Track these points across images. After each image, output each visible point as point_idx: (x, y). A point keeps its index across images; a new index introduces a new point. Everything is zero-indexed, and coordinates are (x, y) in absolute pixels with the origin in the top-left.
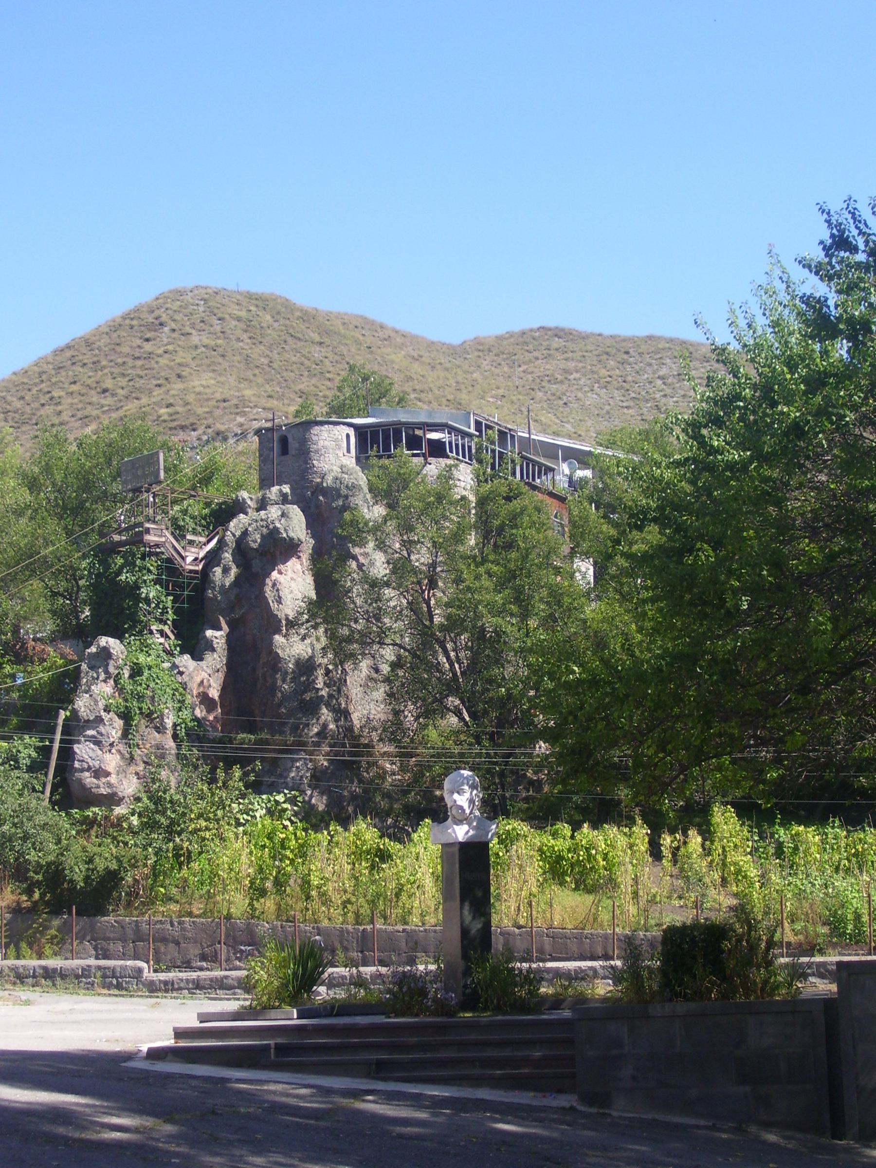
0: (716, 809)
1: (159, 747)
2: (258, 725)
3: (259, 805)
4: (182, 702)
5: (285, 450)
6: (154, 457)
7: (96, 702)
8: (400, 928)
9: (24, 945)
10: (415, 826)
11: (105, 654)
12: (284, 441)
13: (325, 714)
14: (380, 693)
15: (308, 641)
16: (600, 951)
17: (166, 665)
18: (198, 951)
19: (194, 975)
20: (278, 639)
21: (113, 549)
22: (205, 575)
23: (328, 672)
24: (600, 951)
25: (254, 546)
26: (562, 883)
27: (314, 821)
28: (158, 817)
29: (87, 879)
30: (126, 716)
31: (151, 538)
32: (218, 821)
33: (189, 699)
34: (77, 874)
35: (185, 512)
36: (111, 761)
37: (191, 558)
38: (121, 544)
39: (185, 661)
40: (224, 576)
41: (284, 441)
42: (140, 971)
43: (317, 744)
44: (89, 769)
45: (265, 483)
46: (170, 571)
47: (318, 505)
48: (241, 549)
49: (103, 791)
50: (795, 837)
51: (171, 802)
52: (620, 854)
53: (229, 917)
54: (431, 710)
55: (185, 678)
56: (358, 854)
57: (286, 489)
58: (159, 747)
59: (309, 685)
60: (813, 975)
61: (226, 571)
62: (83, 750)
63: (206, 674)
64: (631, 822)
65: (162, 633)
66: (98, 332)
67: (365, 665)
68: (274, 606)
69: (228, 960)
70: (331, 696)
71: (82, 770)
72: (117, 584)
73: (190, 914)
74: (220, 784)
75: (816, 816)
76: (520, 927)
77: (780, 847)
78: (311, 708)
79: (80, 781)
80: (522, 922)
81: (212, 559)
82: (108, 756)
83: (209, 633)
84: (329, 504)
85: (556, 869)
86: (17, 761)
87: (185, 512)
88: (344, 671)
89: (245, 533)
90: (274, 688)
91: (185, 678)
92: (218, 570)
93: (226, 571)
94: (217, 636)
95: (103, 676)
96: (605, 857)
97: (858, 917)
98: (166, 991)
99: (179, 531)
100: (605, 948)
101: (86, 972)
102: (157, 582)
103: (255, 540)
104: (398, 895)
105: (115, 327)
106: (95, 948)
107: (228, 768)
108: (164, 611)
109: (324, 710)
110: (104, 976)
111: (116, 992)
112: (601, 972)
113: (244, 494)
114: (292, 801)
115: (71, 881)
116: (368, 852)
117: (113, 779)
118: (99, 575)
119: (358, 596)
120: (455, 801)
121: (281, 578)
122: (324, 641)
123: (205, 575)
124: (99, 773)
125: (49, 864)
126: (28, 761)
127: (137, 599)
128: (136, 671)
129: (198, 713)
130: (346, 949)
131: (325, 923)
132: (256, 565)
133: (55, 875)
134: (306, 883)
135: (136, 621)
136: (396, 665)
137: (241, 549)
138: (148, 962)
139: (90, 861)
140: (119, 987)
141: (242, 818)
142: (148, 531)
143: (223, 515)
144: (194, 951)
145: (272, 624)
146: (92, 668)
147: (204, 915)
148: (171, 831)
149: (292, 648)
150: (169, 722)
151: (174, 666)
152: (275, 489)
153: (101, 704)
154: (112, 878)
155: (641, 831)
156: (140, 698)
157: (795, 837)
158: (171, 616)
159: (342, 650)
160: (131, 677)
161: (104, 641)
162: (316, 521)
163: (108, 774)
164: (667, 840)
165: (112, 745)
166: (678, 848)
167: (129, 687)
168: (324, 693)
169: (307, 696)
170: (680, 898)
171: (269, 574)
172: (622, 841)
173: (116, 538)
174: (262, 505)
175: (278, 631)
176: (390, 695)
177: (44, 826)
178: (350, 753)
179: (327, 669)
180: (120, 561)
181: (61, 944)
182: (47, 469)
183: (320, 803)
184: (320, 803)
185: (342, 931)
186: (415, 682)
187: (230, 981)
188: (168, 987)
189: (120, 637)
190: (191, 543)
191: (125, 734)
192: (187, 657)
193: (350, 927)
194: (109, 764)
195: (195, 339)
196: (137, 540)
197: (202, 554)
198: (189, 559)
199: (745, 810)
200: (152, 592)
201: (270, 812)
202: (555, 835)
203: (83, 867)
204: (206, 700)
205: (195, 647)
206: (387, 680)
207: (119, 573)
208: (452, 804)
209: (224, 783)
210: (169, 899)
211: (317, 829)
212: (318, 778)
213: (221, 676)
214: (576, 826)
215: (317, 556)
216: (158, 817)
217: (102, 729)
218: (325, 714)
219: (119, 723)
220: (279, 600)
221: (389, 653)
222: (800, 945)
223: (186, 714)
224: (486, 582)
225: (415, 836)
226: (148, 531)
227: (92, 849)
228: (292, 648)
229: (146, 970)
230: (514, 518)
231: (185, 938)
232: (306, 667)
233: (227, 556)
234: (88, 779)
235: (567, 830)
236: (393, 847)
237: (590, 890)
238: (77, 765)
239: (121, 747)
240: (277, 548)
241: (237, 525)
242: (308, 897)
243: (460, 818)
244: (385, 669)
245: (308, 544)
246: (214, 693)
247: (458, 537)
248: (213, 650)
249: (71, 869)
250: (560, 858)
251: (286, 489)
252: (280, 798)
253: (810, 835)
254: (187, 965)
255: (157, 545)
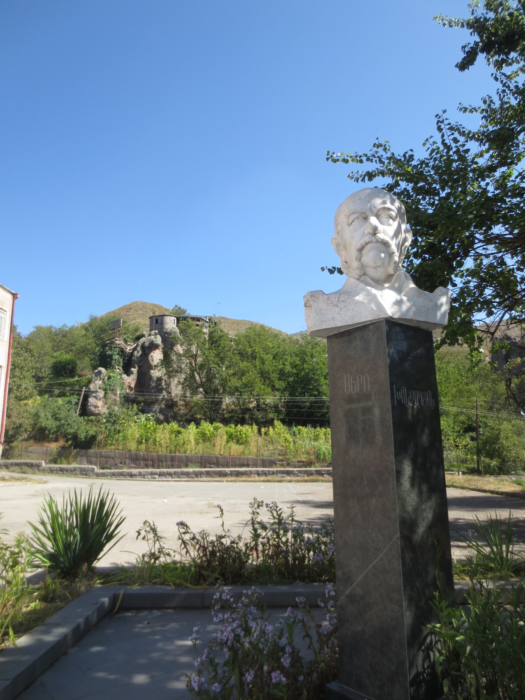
0: (276, 421)
1: (115, 400)
2: (145, 396)
3: (143, 417)
4: (123, 387)
5: (157, 322)
6: (119, 321)
7: (96, 386)
8: (184, 455)
9: (63, 458)
10: (189, 424)
11: (100, 372)
12: (157, 320)
13: (164, 393)
14: (180, 387)
15: (160, 372)
16: (246, 463)
17: (119, 377)
18: (120, 461)
19: (113, 471)
20: (152, 371)
21: (106, 345)
22: (132, 354)
23: (166, 381)
24: (246, 463)
25: (147, 346)
26: (233, 441)
27: (159, 422)
28: (110, 419)
29: (86, 438)
30: (105, 390)
31: (118, 342)
32: (128, 420)
33: (125, 387)
34: (82, 436)
35: (128, 337)
36: (100, 403)
37: (129, 349)
38: (109, 344)
39: (124, 376)
40: (138, 354)
41: (157, 320)
42: (93, 469)
43: (162, 401)
44: (93, 405)
45: (151, 330)
46: (122, 352)
47: (165, 337)
48: (143, 347)
49: (97, 412)
50: (299, 430)
51: (115, 415)
52: (250, 434)
53: (130, 450)
54: (194, 392)
55: (124, 381)
56: (172, 432)
57: (157, 331)
58: (115, 400)
59: (160, 384)
60: (325, 474)
61: (138, 352)
62: (91, 400)
63: (131, 380)
64: (252, 425)
65: (118, 369)
66: (116, 310)
67: (176, 380)
68: (151, 362)
69: (129, 464)
70: (166, 388)
71: (91, 406)
72: (105, 354)
73: (118, 449)
74: (130, 409)
75: (304, 424)
76: (221, 455)
77: (294, 432)
78: (160, 391)
79: (90, 409)
80: (222, 453)
81: (135, 349)
82: (99, 402)
83: (132, 369)
84: (168, 337)
85: (230, 437)
86: (71, 402)
87: (128, 337)
88: (170, 382)
89: (144, 342)
90: (150, 385)
91: (124, 381)
92: (136, 352)
93: (138, 352)
94: (135, 370)
95: (99, 379)
96: (245, 434)
97: (324, 454)
98: (103, 476)
99: (126, 341)
100: (247, 462)
101: (75, 469)
102: (118, 354)
103: (147, 344)
104: (183, 445)
105: (120, 309)
106: (87, 460)
107: (132, 404)
108: (120, 363)
109: (164, 391)
110: (81, 471)
111: (85, 476)
112: (253, 472)
113: (145, 333)
114: (153, 416)
115: (80, 438)
116: (175, 431)
117: (100, 409)
118: (102, 352)
119: (174, 358)
120: (375, 231)
121: (154, 355)
122: (164, 371)
123: (132, 354)
124: (96, 407)
125: (74, 433)
126: (74, 403)
127: (112, 359)
128: (109, 378)
129: (128, 391)
130: (166, 461)
131: (160, 453)
132: (147, 351)
133: (75, 437)
134: (155, 440)
135: (111, 365)
136: (185, 379)
137: (143, 347)
138: (97, 466)
139: (87, 432)
140: (86, 474)
141: (138, 421)
142: (116, 340)
143: (138, 338)
144: (118, 461)
145: (150, 367)
146: (96, 376)
147: (122, 450)
148: (114, 423)
149: (156, 373)
150: (118, 392)
151: (121, 378)
152: (153, 331)
153: (98, 387)
154: (93, 438)
155: (255, 427)
156: (110, 385)
157: (299, 430)
158: (121, 364)
159: (170, 374)
160: (108, 379)
161: (100, 369)
162: (164, 341)
163: (98, 407)
164: (263, 430)
165: (100, 399)
166: (266, 432)
167: (107, 382)
168: (164, 387)
169: (160, 387)
170: (267, 447)
171: (150, 354)
172: (250, 430)
173: (107, 342)
174: (150, 335)
175: (152, 369)
176: (183, 388)
177: (74, 421)
178: (171, 404)
179: (166, 381)
180: (108, 348)
181: (75, 457)
182: (91, 325)
183: (161, 417)
184: (161, 417)
185: (165, 456)
186: (190, 384)
187: (125, 473)
188: (103, 475)
189: (106, 369)
190: (129, 345)
191: (105, 397)
192: (125, 375)
193: (168, 454)
194: (98, 404)
195: (139, 312)
196: (113, 343)
197: (132, 348)
198: (128, 349)
199: (283, 422)
200: (116, 357)
201: (146, 419)
202: (230, 427)
203: (85, 434)
204: (130, 387)
205: (128, 372)
206: (183, 384)
207: (107, 351)
208: (367, 239)
209: (132, 410)
210: (112, 444)
211: (160, 424)
212: (161, 412)
213: (135, 381)
214: (236, 426)
215: (163, 349)
216: (110, 419)
217: (97, 394)
218: (164, 393)
219: (103, 392)
220: (153, 361)
221: (183, 376)
222: (307, 462)
223: (123, 391)
224: (212, 354)
225: (189, 427)
226: (116, 340)
227: (88, 428)
228: (156, 373)
229: (96, 469)
230: (220, 337)
231: (116, 457)
232: (159, 379)
233: (139, 348)
234: (92, 409)
235: (233, 426)
236: (182, 430)
237: (241, 444)
238: (89, 404)
239: (103, 399)
240: (153, 346)
241: (142, 340)
242: (155, 445)
243: (379, 274)
244: (182, 380)
245: (162, 346)
246: (133, 386)
247: (204, 344)
248: (133, 374)
249: (80, 434)
250: (232, 434)
251: (157, 331)
252: (149, 415)
253: (304, 429)
254: (116, 466)
255: (119, 345)
